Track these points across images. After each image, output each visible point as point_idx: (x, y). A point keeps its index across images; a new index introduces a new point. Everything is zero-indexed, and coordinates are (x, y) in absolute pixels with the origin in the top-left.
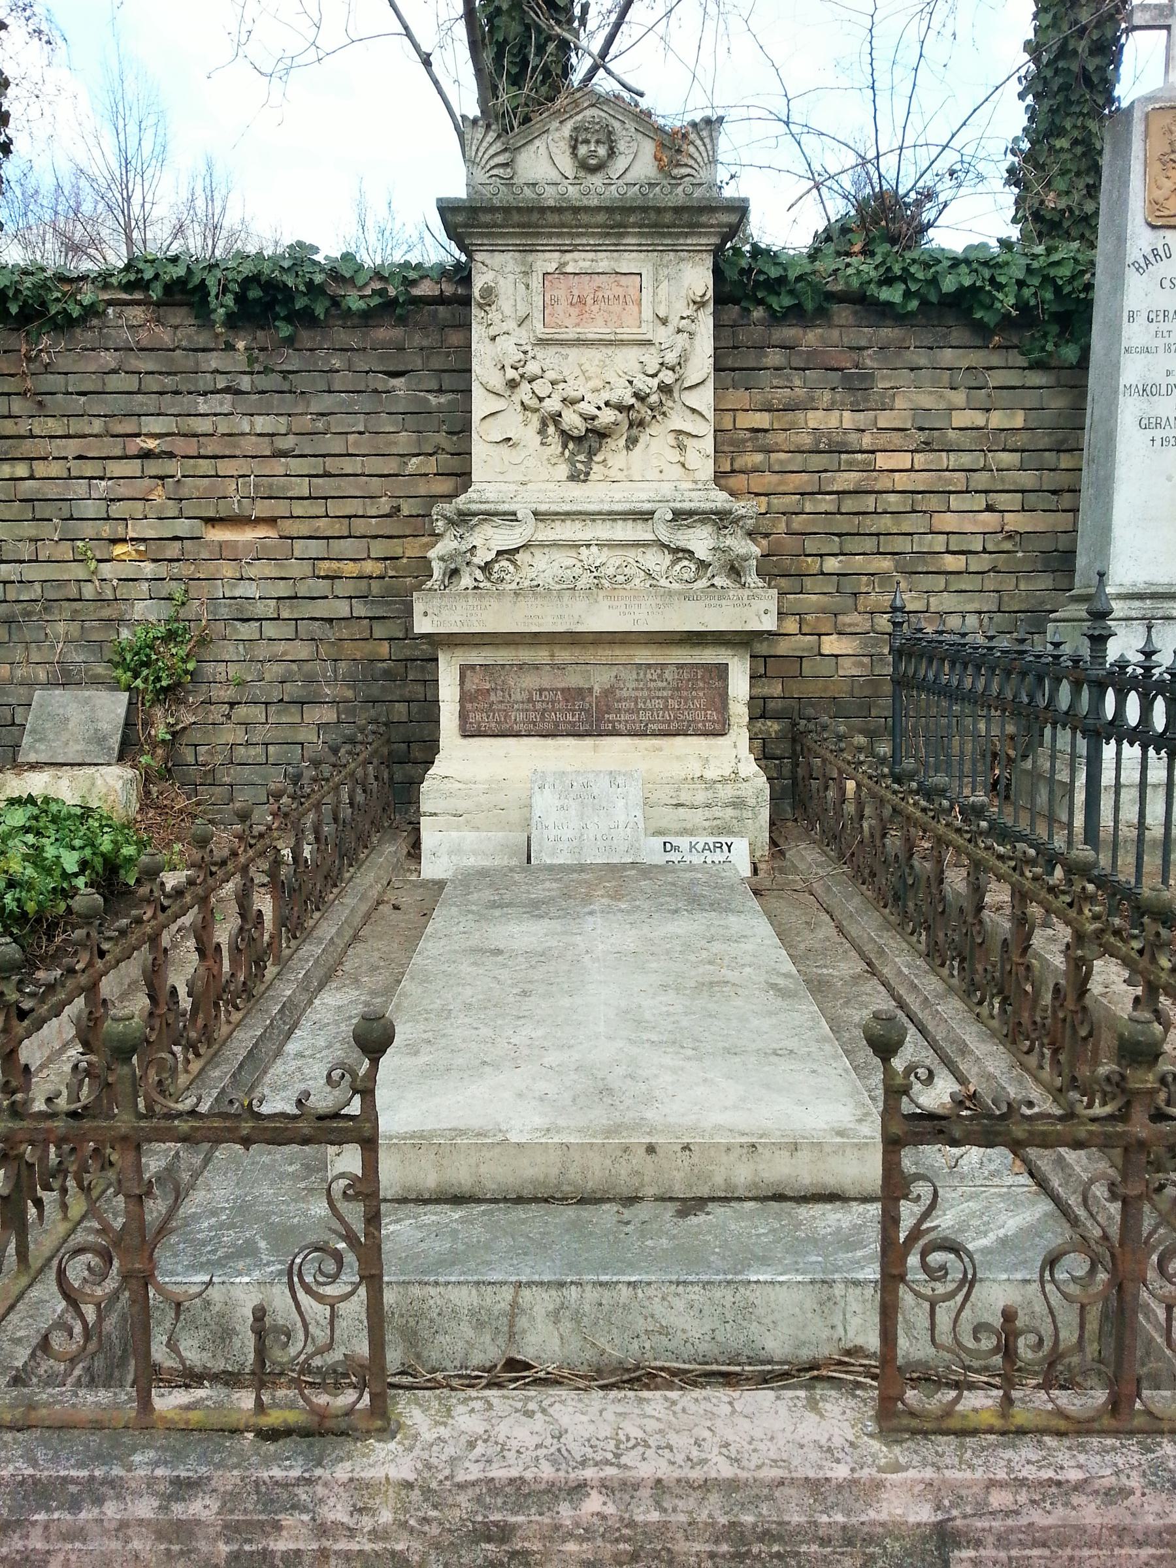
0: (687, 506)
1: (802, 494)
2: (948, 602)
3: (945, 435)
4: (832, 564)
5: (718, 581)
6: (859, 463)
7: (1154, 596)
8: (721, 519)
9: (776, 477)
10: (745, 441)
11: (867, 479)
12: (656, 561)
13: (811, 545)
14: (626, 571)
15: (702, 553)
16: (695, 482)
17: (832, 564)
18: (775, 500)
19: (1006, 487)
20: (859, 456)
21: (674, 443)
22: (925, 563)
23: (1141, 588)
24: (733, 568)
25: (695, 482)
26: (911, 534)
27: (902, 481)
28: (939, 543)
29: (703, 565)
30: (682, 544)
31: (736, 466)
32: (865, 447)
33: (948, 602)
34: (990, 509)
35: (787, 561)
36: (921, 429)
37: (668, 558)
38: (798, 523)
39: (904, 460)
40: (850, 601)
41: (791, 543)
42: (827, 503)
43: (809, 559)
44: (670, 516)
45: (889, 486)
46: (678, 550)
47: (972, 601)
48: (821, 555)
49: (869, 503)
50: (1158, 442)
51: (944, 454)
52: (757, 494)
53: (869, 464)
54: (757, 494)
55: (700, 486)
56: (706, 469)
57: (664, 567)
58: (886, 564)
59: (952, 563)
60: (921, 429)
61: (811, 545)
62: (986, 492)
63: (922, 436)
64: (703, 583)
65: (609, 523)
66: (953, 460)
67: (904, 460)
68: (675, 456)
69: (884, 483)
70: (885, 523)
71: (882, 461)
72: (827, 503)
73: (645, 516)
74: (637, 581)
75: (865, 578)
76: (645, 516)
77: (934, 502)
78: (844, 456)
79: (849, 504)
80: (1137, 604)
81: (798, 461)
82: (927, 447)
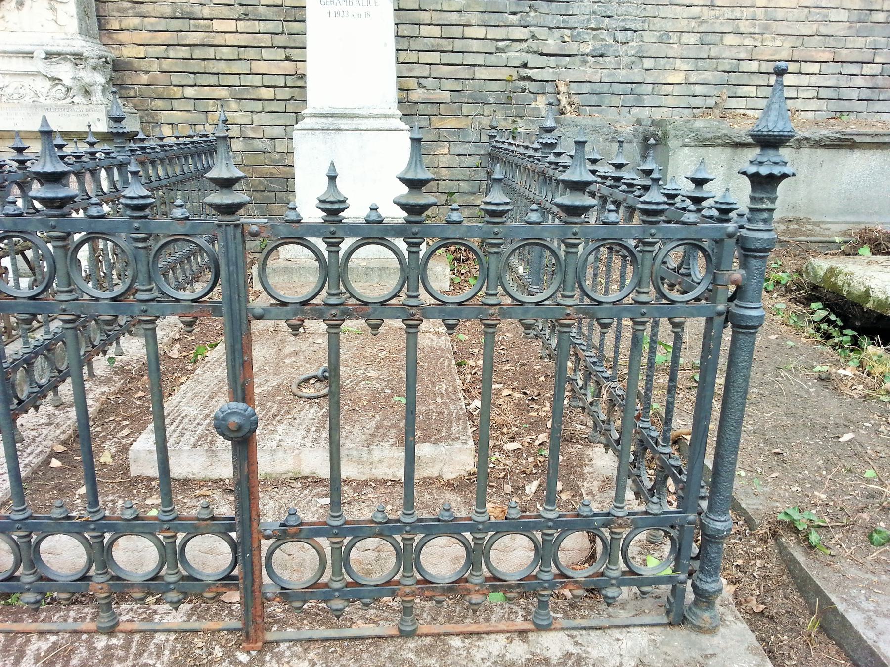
0: (55, 49)
1: (168, 46)
2: (265, 118)
3: (256, 10)
4: (190, 92)
5: (76, 100)
6: (202, 26)
7: (333, 116)
8: (78, 58)
9: (149, 34)
10: (126, 9)
11: (208, 37)
12: (42, 85)
13: (176, 79)
14: (22, 92)
15: (68, 82)
16: (66, 34)
17: (190, 92)
18: (149, 49)
19: (297, 45)
20: (202, 22)
21: (48, 6)
22: (249, 93)
23: (326, 110)
24: (86, 91)
25: (66, 34)
26: (239, 74)
27: (231, 39)
28: (256, 80)
29: (69, 90)
30: (55, 75)
31: (123, 27)
32: (205, 16)
33: (265, 118)
34: (288, 59)
35: (161, 89)
36: (242, 5)
37: (48, 84)
38: (166, 65)
39: (231, 26)
40: (203, 116)
41: (163, 78)
42: (184, 52)
43: (175, 88)
44: (44, 56)
45: (223, 43)
46: (54, 79)
47: (280, 118)
48: (183, 86)
49: (210, 53)
50: (332, 14)
51: (256, 22)
52: (139, 45)
53: (209, 27)
54: (139, 45)
55: (69, 37)
56: (73, 25)
57: (47, 90)
58: (223, 93)
59: (266, 93)
60: (242, 5)
61: (176, 79)
62: (285, 48)
63: (242, 10)
64: (68, 100)
65: (7, 59)
66: (263, 26)
67: (231, 26)
68: (50, 15)
69: (218, 39)
70: (221, 66)
71: (217, 25)
72: (184, 52)
73: (29, 55)
74: (27, 98)
75: (211, 102)
76: (29, 55)
77: (251, 53)
78: (192, 21)
79: (198, 53)
80: (323, 120)
81: (162, 24)
82: (245, 17)
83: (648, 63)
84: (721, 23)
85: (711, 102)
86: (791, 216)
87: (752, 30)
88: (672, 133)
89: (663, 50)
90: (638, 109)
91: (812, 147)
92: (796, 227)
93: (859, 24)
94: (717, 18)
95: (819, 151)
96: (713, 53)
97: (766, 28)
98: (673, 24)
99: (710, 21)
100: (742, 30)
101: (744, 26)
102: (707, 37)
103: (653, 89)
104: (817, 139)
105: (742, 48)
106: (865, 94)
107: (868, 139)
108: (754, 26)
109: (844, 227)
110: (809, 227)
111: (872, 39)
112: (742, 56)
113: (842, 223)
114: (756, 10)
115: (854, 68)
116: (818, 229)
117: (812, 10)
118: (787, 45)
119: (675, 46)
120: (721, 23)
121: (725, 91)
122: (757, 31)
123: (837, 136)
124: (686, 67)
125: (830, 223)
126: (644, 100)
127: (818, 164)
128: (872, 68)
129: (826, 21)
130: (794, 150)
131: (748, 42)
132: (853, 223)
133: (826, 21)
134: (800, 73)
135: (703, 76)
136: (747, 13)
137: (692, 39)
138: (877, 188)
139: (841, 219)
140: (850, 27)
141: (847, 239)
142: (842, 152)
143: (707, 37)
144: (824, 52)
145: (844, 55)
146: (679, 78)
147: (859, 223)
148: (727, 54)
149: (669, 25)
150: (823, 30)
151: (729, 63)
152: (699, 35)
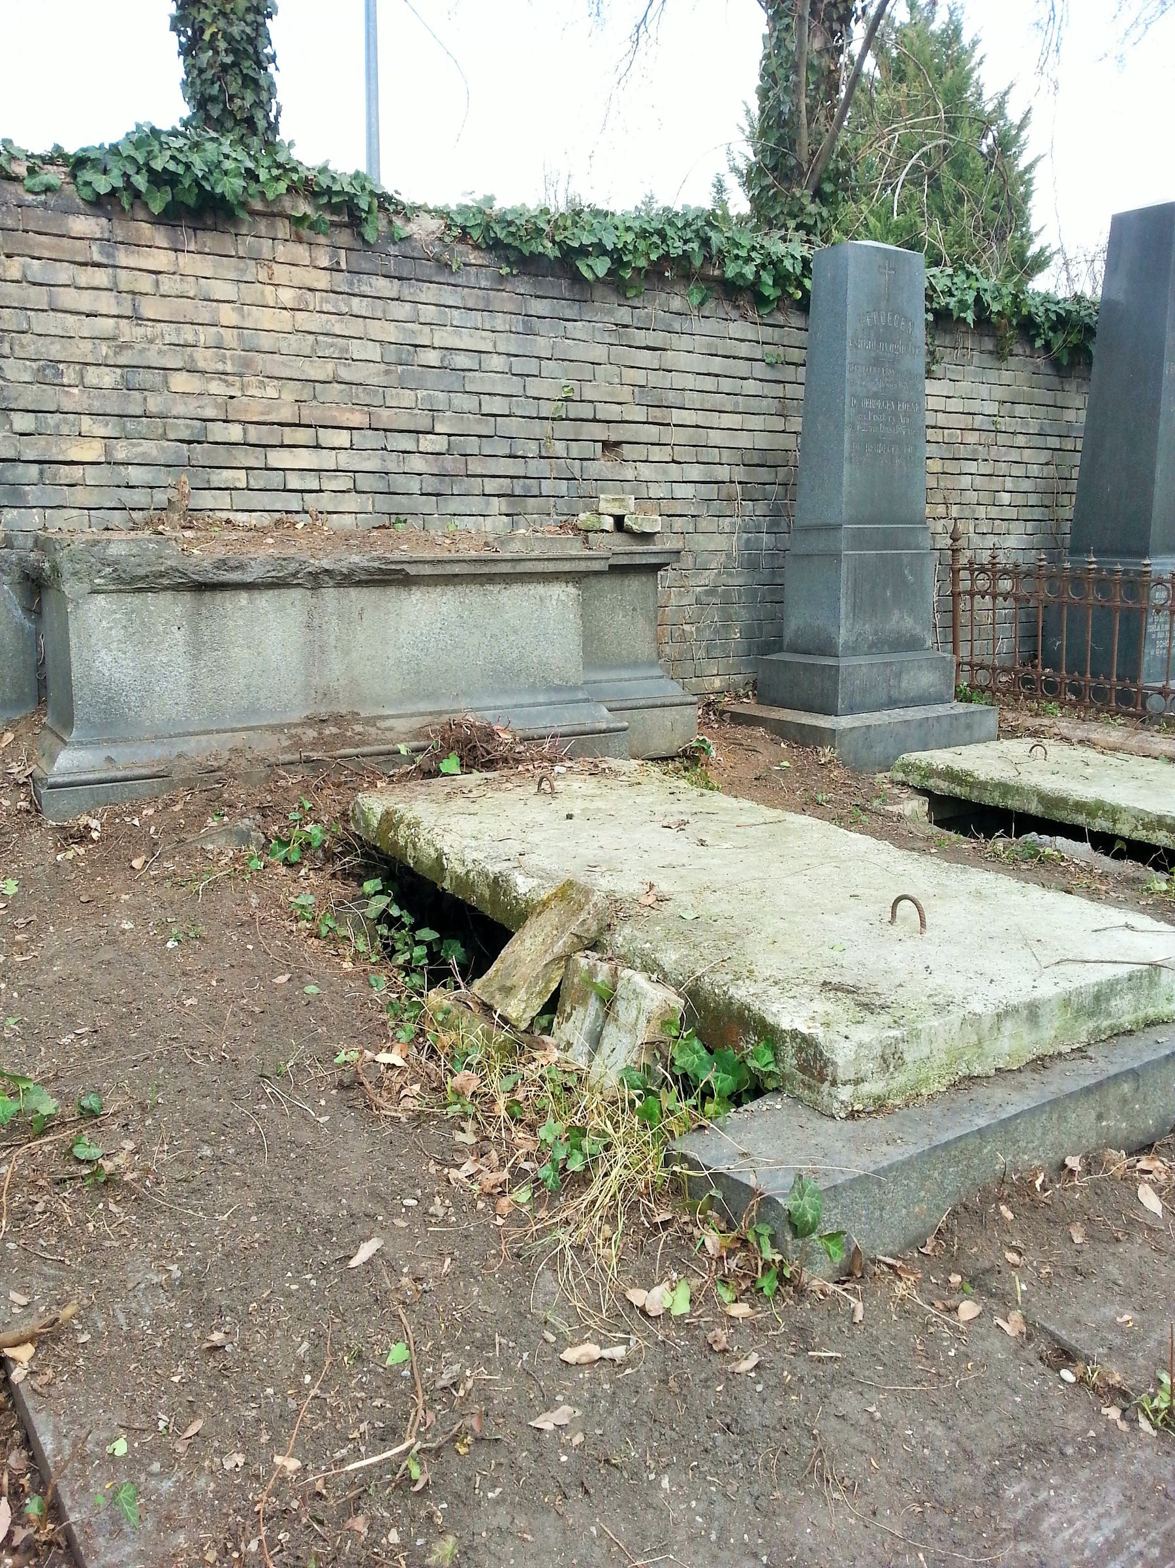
83: (23, 422)
84: (160, 352)
85: (161, 497)
86: (323, 711)
87: (220, 367)
88: (66, 567)
89: (49, 397)
90: (15, 512)
91: (339, 585)
92: (334, 730)
93: (400, 368)
94: (151, 341)
95: (353, 592)
96: (154, 404)
97: (247, 364)
98: (64, 348)
99: (138, 347)
100: (201, 365)
101: (204, 359)
102: (132, 377)
103: (41, 472)
104: (345, 571)
105: (206, 400)
106: (431, 485)
107: (427, 570)
108: (223, 360)
109: (416, 723)
110: (358, 728)
111: (425, 392)
112: (210, 413)
113: (412, 715)
114: (222, 330)
115: (405, 442)
116: (372, 730)
117: (320, 338)
118: (288, 397)
119: (75, 391)
120: (160, 352)
121: (184, 478)
122: (229, 369)
123: (376, 564)
124: (103, 432)
125: (393, 717)
126: (26, 493)
127: (356, 616)
128: (432, 442)
129: (345, 359)
130: (309, 593)
131: (216, 387)
132: (431, 713)
133: (345, 359)
134: (318, 447)
135: (140, 449)
136: (206, 335)
137: (108, 378)
138: (459, 652)
139: (410, 708)
140: (387, 372)
141: (422, 743)
142: (392, 591)
143: (132, 377)
144: (352, 411)
145: (385, 417)
146: (92, 451)
147: (440, 713)
148: (179, 409)
149: (55, 350)
150: (344, 374)
151: (187, 426)
152: (118, 371)
